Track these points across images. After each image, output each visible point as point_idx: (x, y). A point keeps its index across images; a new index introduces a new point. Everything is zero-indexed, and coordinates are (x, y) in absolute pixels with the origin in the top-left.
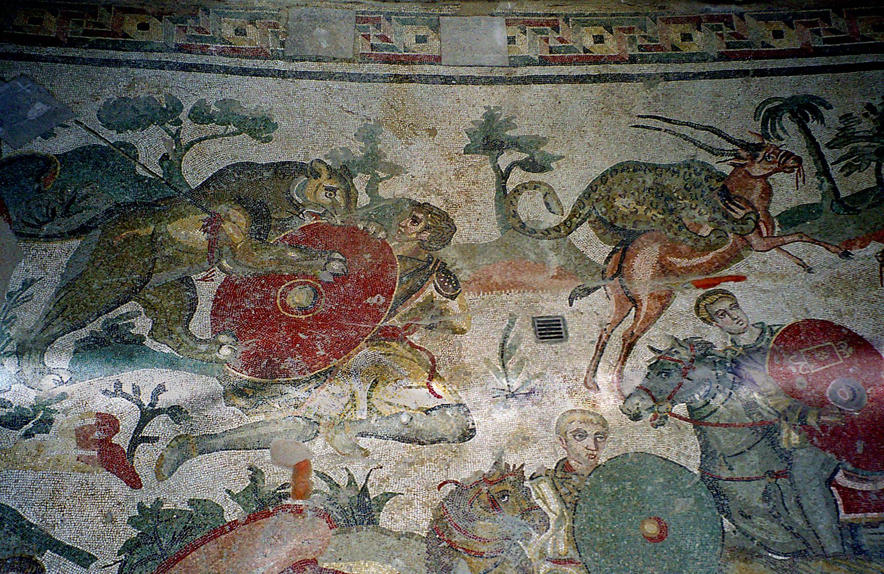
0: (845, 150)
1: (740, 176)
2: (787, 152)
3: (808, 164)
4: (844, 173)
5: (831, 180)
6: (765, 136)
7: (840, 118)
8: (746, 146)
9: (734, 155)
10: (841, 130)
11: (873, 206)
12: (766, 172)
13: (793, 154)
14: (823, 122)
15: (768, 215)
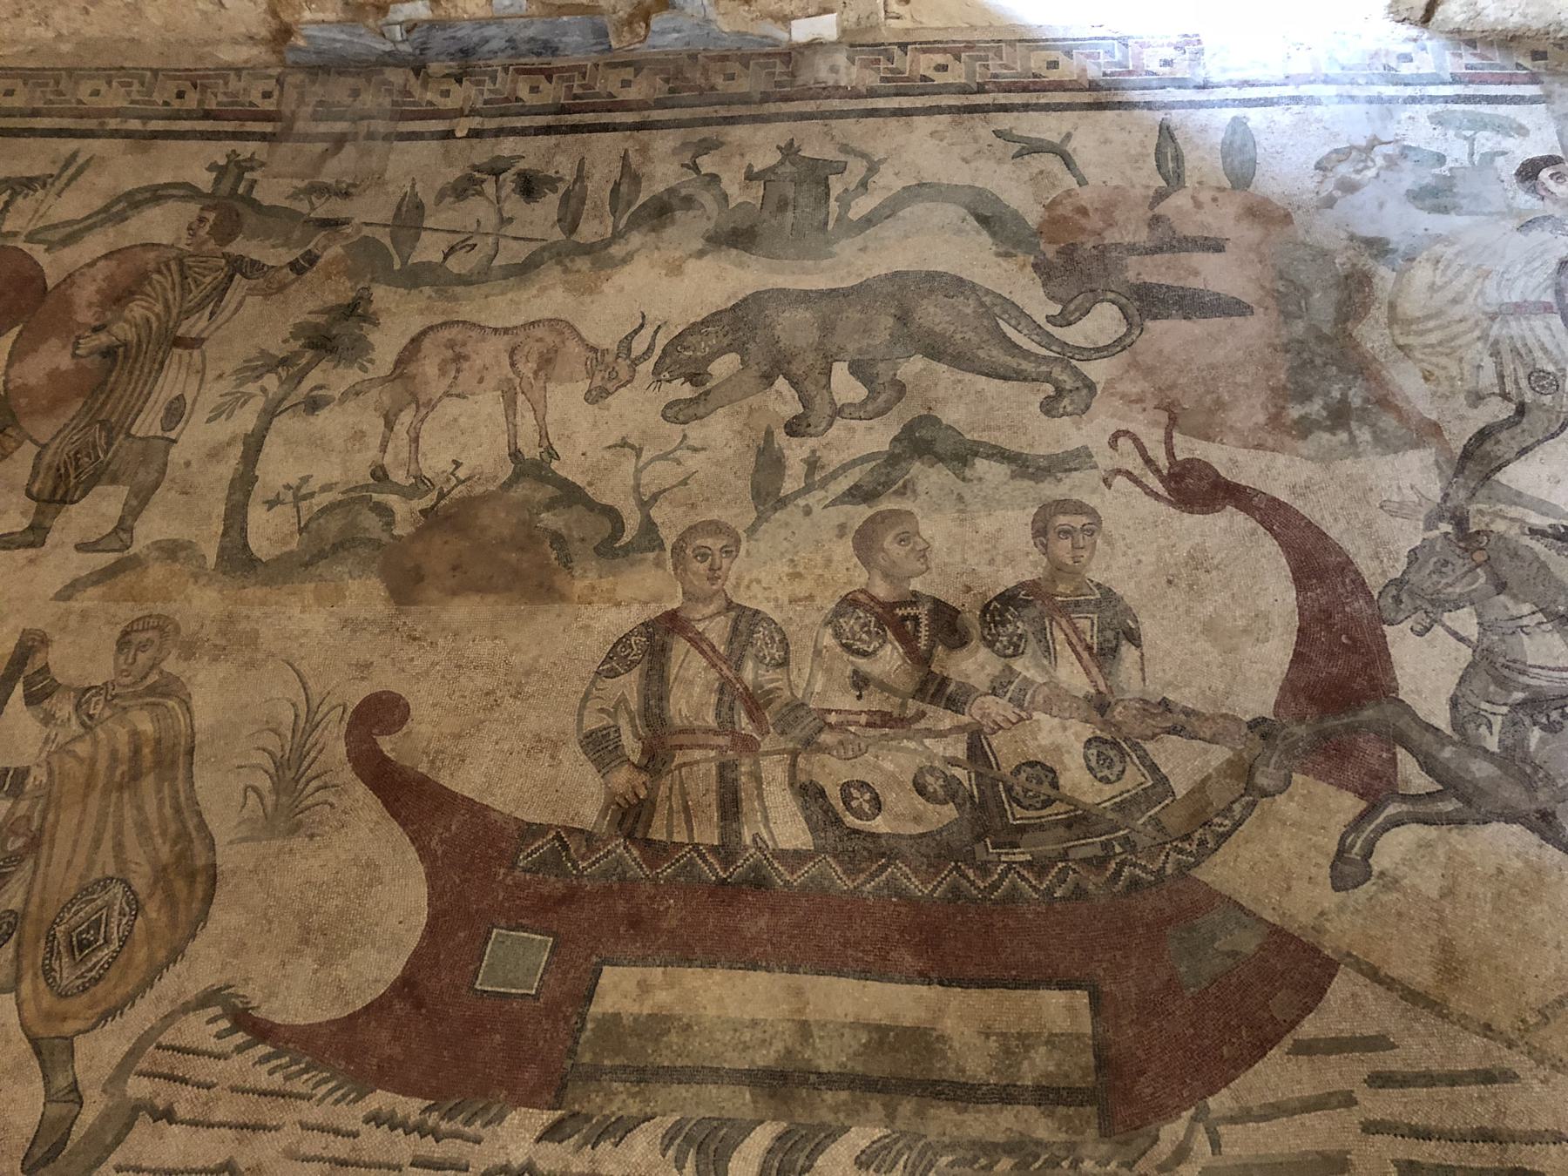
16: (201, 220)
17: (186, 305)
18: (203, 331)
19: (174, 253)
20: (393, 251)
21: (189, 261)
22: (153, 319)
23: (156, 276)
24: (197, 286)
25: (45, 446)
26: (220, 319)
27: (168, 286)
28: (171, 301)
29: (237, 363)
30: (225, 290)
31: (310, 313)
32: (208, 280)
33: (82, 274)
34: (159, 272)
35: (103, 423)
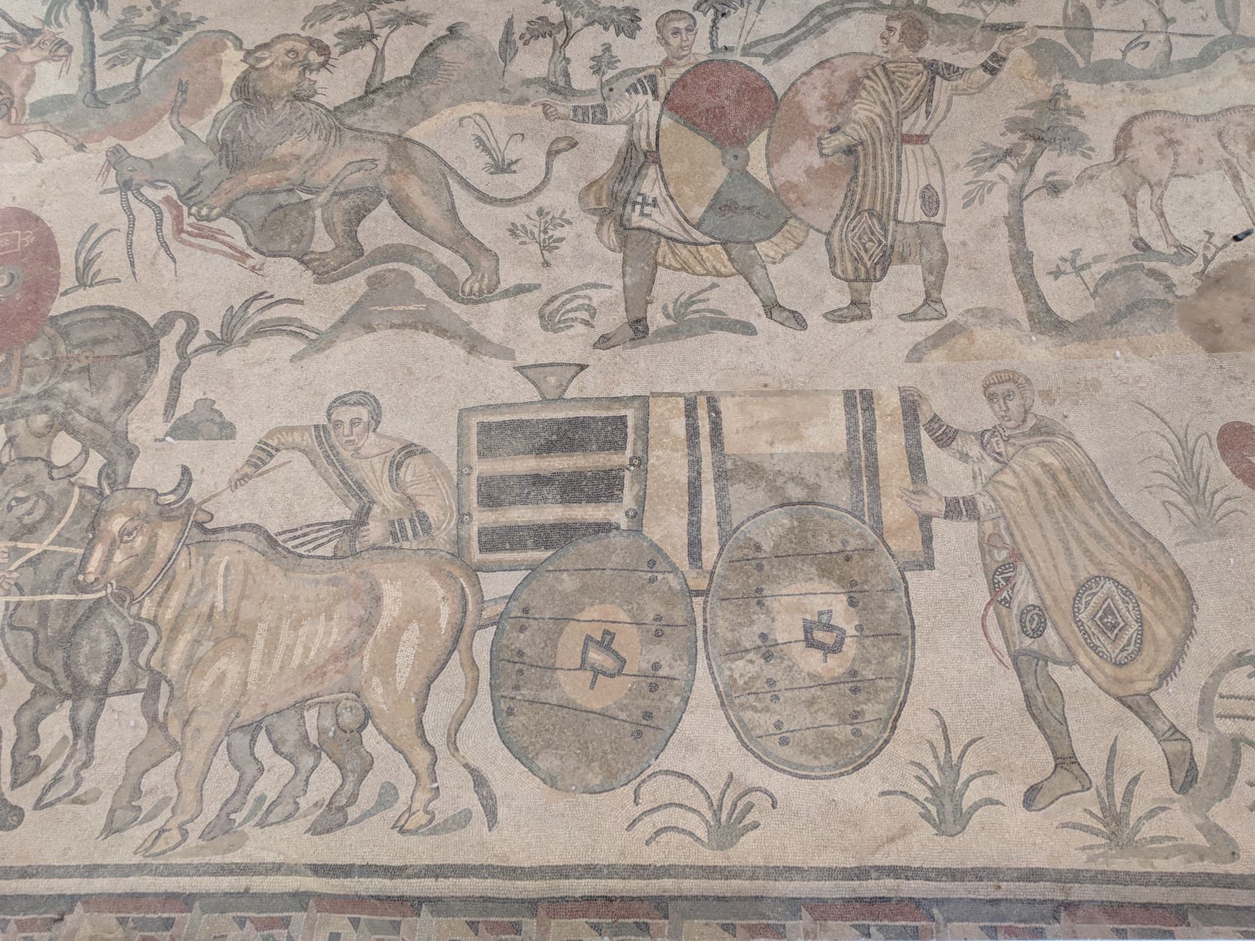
0: (117, 43)
1: (10, 61)
2: (62, 40)
3: (78, 55)
4: (108, 66)
5: (93, 72)
6: (47, 22)
7: (124, 10)
8: (24, 30)
9: (11, 39)
10: (121, 22)
11: (123, 101)
12: (35, 59)
13: (67, 42)
14: (106, 12)
15: (23, 104)
16: (890, 29)
17: (901, 107)
18: (925, 128)
19: (876, 60)
20: (1072, 51)
21: (890, 67)
22: (877, 120)
23: (867, 82)
24: (906, 89)
25: (829, 234)
26: (937, 116)
27: (880, 89)
28: (888, 104)
29: (967, 157)
30: (931, 92)
31: (1017, 109)
32: (913, 83)
33: (803, 83)
34: (868, 77)
35: (871, 212)
